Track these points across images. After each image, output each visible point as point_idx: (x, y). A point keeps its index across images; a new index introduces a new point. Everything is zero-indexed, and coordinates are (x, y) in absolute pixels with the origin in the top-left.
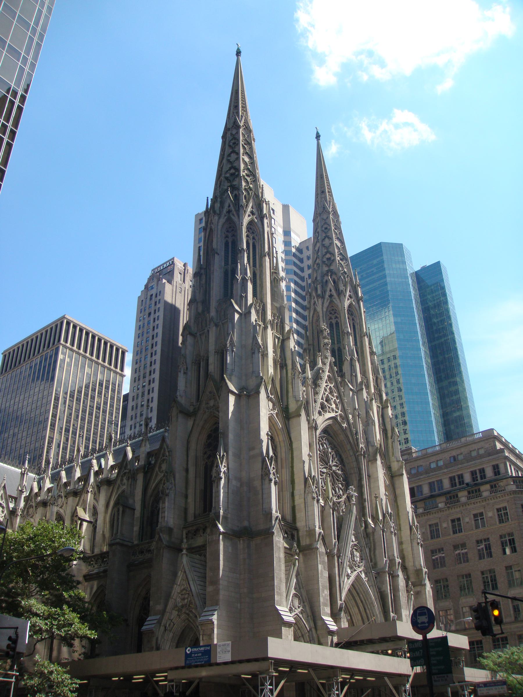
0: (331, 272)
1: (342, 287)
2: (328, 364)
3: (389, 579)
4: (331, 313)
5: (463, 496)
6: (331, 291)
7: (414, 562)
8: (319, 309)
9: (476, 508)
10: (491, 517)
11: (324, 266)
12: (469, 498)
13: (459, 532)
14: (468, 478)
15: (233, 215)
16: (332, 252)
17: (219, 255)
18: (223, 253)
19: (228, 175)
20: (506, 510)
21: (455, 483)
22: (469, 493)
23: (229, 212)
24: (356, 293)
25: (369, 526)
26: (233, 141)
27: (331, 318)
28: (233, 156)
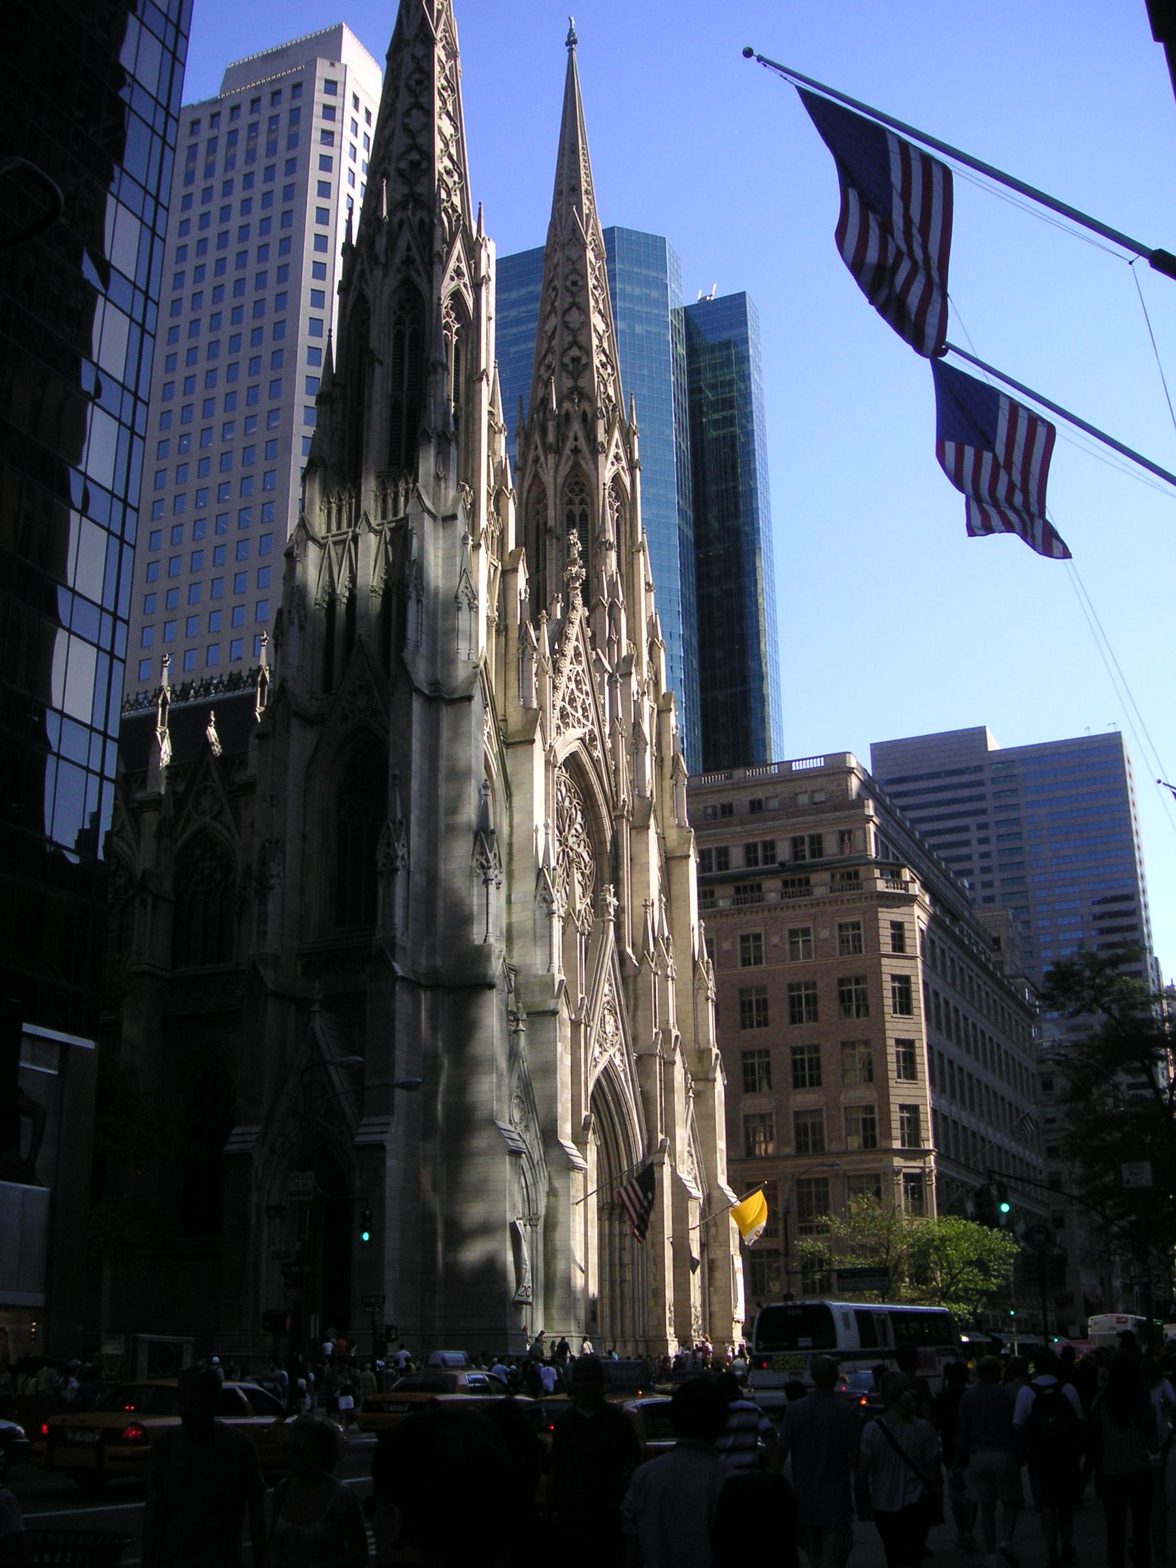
0: (579, 393)
1: (601, 437)
2: (577, 622)
3: (660, 1069)
4: (572, 491)
5: (772, 889)
6: (576, 439)
7: (696, 1033)
8: (548, 478)
9: (796, 918)
10: (826, 940)
11: (564, 374)
12: (784, 895)
13: (756, 963)
14: (783, 852)
15: (417, 271)
16: (584, 344)
17: (381, 364)
18: (388, 361)
19: (403, 165)
20: (859, 929)
21: (756, 858)
22: (785, 884)
23: (408, 261)
24: (629, 451)
25: (628, 961)
26: (417, 76)
27: (571, 502)
28: (417, 116)
